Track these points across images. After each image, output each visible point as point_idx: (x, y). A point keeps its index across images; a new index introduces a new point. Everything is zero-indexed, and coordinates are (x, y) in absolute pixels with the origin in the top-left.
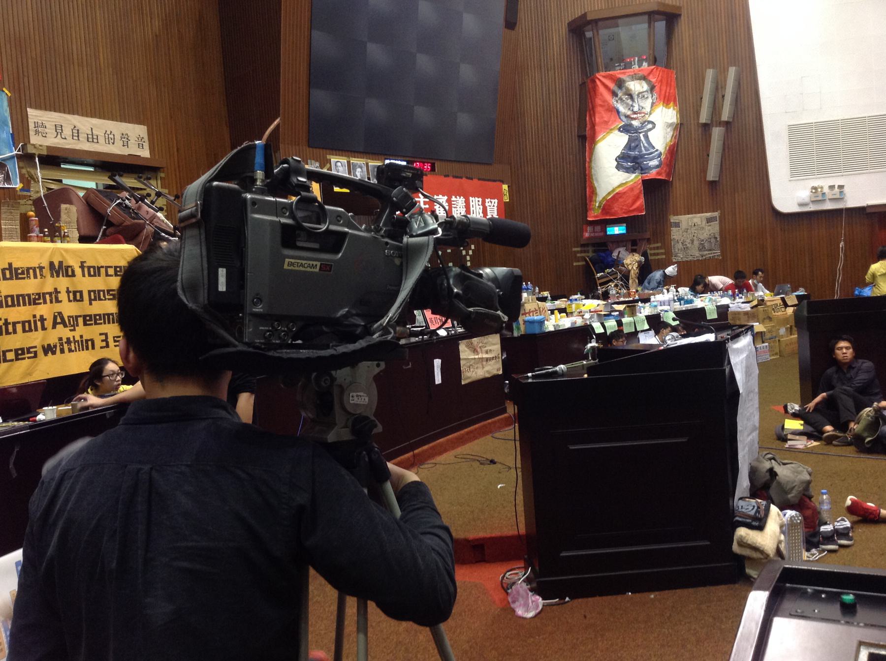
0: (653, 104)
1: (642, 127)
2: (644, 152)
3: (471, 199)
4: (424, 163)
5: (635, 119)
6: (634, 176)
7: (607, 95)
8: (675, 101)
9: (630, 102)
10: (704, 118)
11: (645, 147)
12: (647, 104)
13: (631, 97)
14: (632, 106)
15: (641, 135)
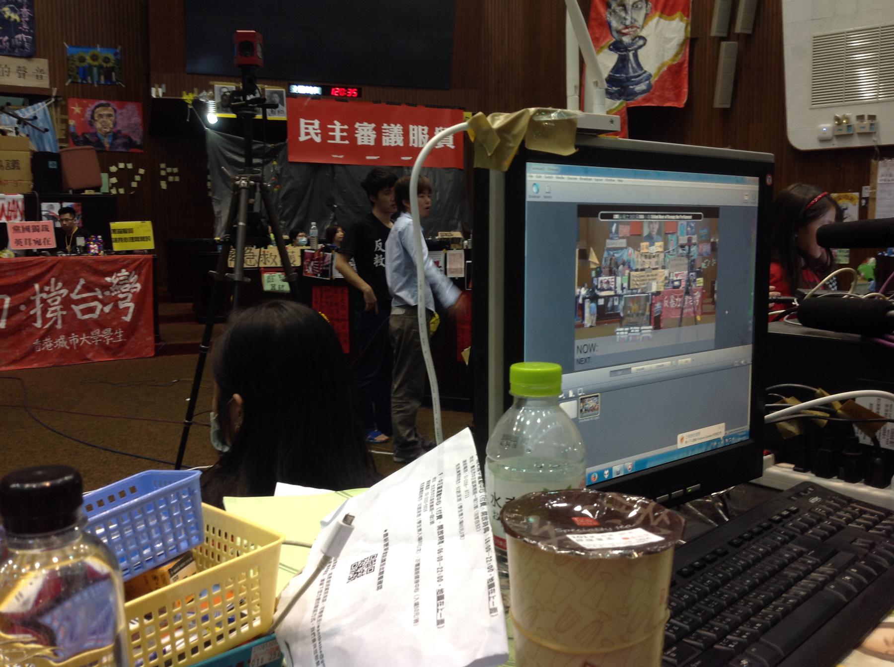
0: (647, 15)
1: (632, 44)
2: (632, 74)
3: (411, 127)
4: (346, 88)
5: (625, 34)
6: (618, 103)
7: (602, 9)
8: (685, 12)
9: (623, 14)
10: (714, 33)
11: (633, 68)
12: (640, 16)
13: (625, 9)
14: (625, 19)
15: (631, 54)
